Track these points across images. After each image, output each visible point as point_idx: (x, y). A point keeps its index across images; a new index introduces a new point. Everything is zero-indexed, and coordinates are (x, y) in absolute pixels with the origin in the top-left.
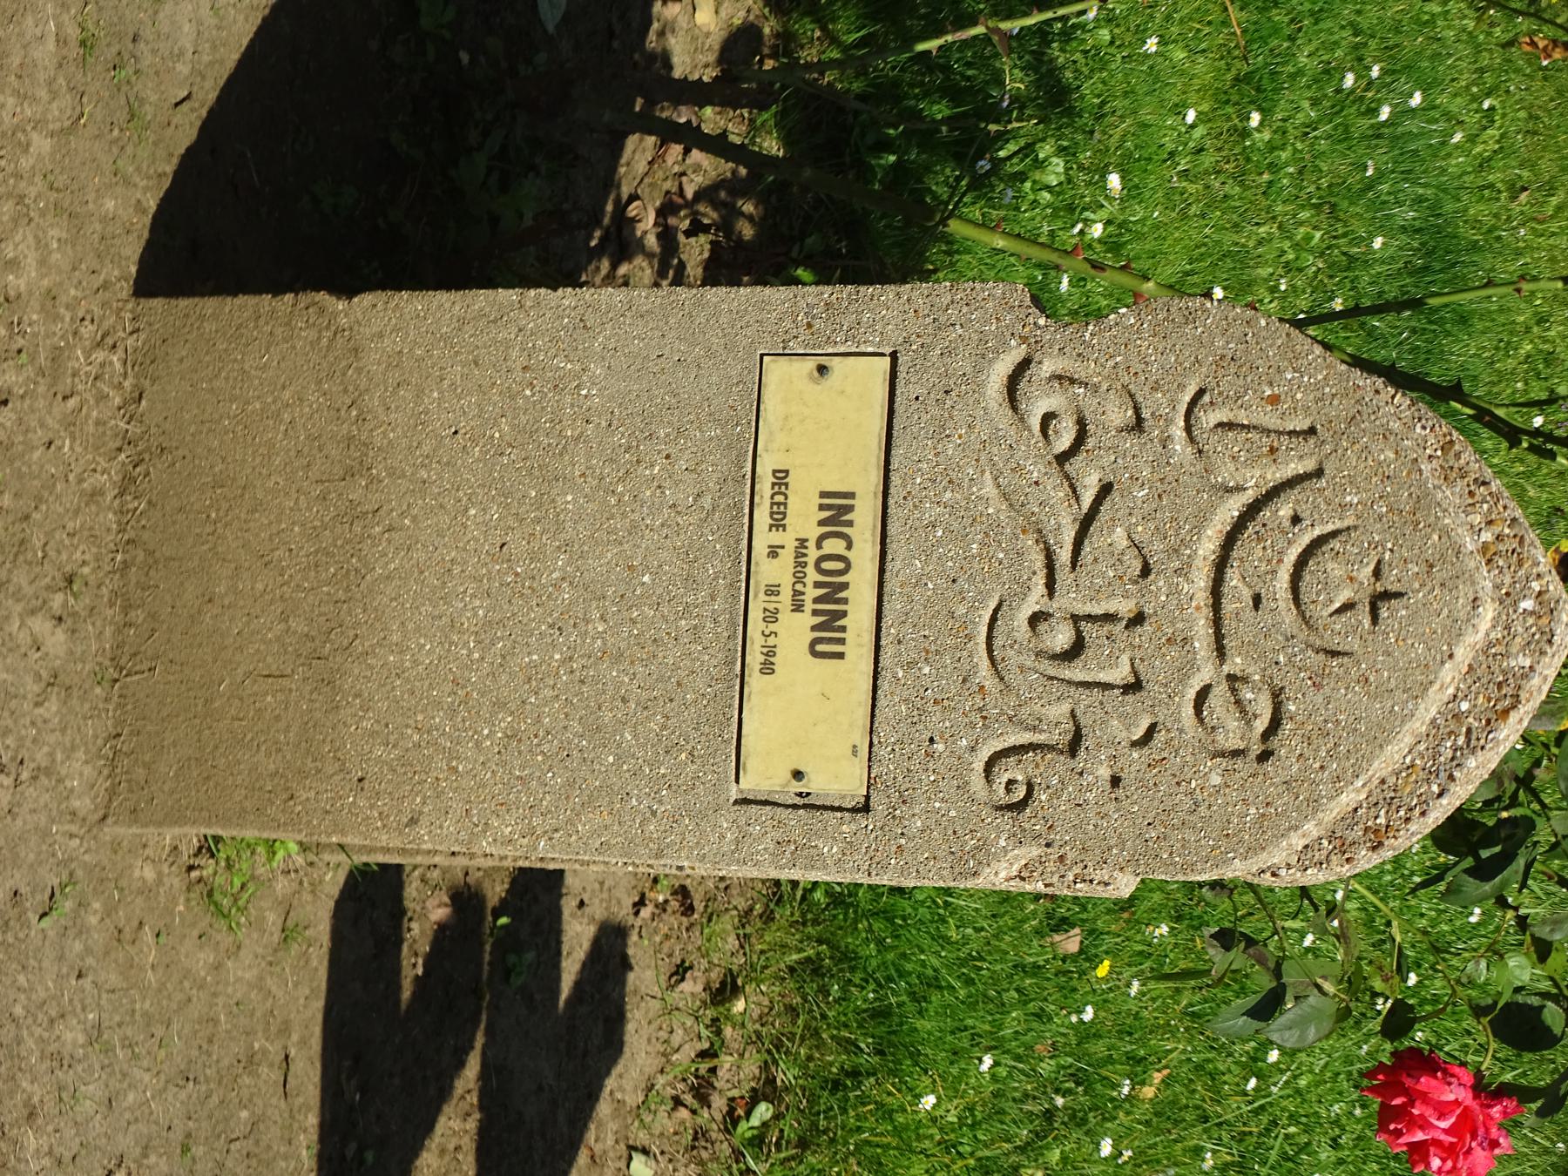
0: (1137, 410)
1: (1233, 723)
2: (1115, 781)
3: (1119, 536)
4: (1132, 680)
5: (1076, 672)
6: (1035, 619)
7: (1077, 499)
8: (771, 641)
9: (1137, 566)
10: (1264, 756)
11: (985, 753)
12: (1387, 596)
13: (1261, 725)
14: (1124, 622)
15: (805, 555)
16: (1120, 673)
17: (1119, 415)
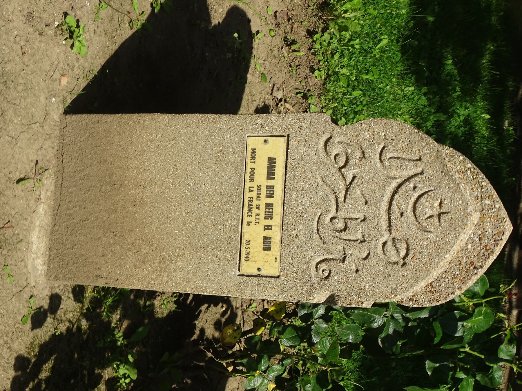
0: (363, 153)
1: (394, 253)
2: (357, 271)
3: (359, 193)
4: (362, 239)
5: (344, 236)
6: (332, 219)
7: (346, 181)
8: (248, 250)
9: (364, 201)
10: (404, 264)
11: (314, 264)
12: (444, 213)
13: (403, 253)
14: (359, 220)
15: (260, 197)
16: (359, 236)
17: (359, 154)
